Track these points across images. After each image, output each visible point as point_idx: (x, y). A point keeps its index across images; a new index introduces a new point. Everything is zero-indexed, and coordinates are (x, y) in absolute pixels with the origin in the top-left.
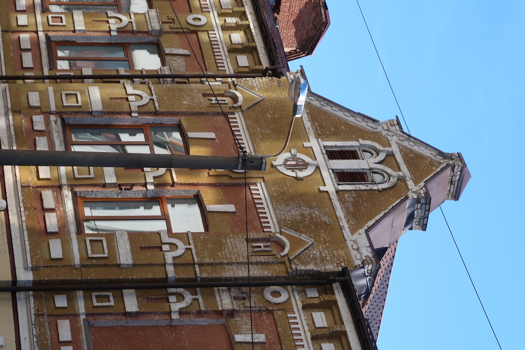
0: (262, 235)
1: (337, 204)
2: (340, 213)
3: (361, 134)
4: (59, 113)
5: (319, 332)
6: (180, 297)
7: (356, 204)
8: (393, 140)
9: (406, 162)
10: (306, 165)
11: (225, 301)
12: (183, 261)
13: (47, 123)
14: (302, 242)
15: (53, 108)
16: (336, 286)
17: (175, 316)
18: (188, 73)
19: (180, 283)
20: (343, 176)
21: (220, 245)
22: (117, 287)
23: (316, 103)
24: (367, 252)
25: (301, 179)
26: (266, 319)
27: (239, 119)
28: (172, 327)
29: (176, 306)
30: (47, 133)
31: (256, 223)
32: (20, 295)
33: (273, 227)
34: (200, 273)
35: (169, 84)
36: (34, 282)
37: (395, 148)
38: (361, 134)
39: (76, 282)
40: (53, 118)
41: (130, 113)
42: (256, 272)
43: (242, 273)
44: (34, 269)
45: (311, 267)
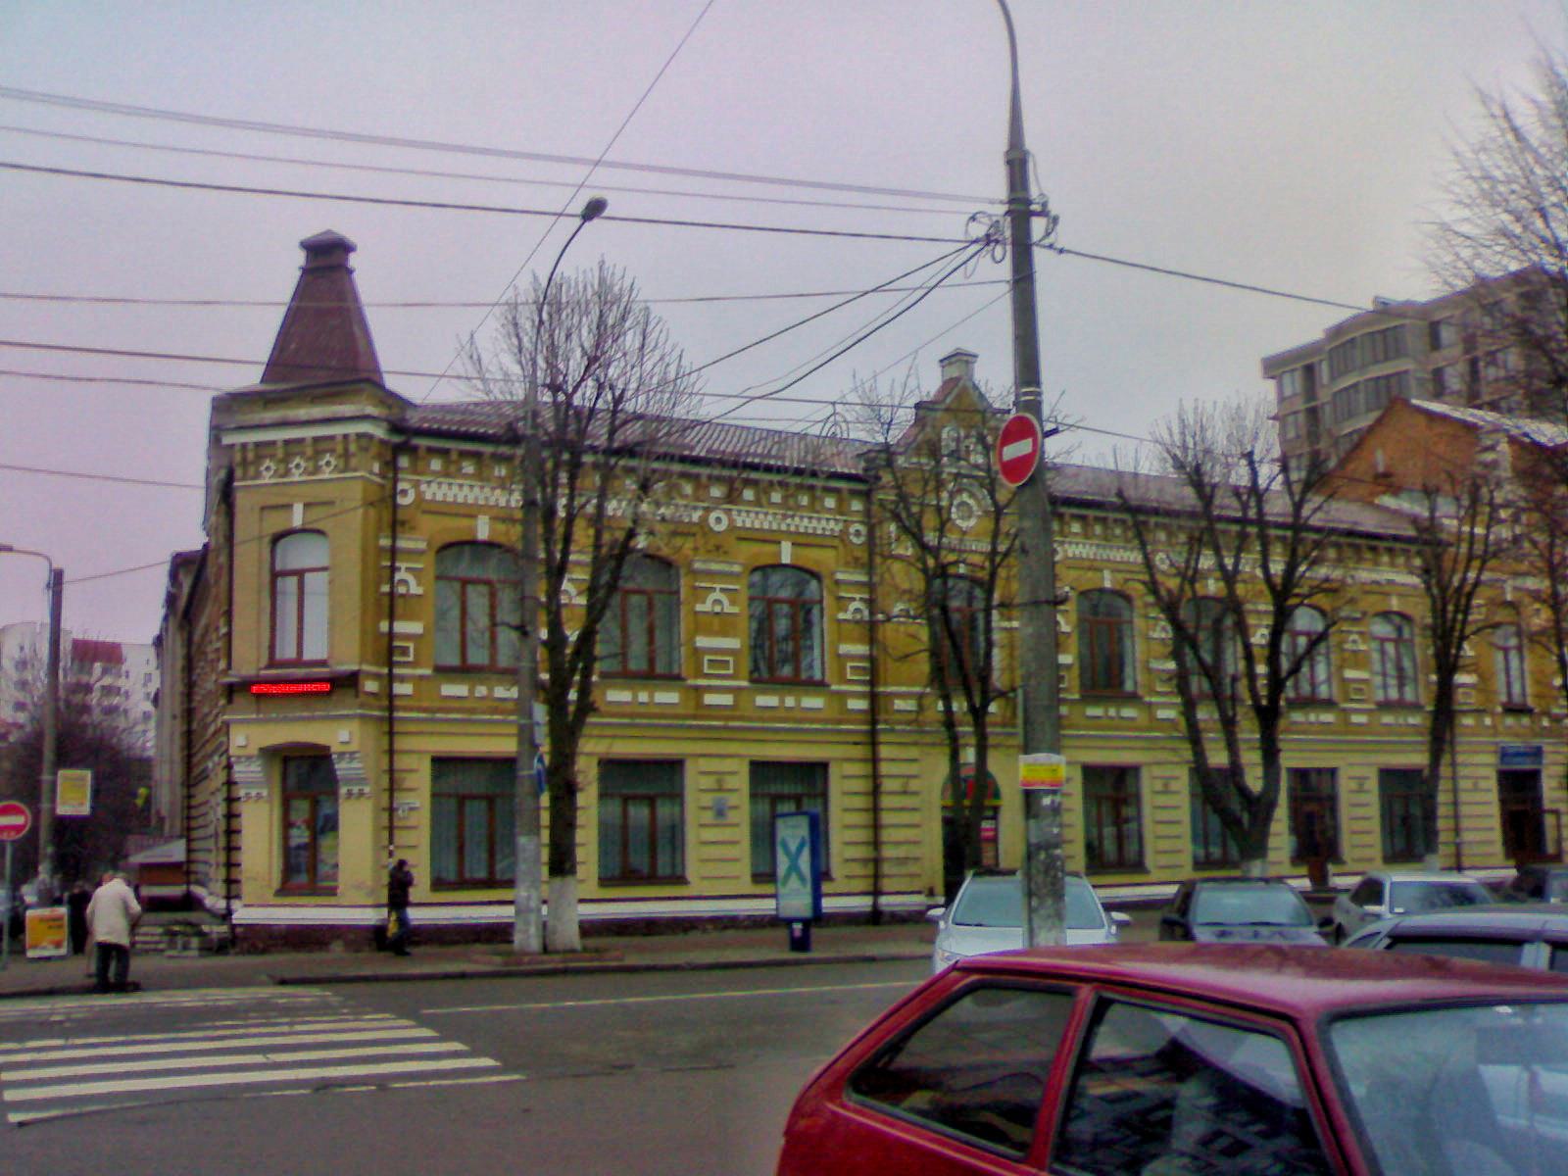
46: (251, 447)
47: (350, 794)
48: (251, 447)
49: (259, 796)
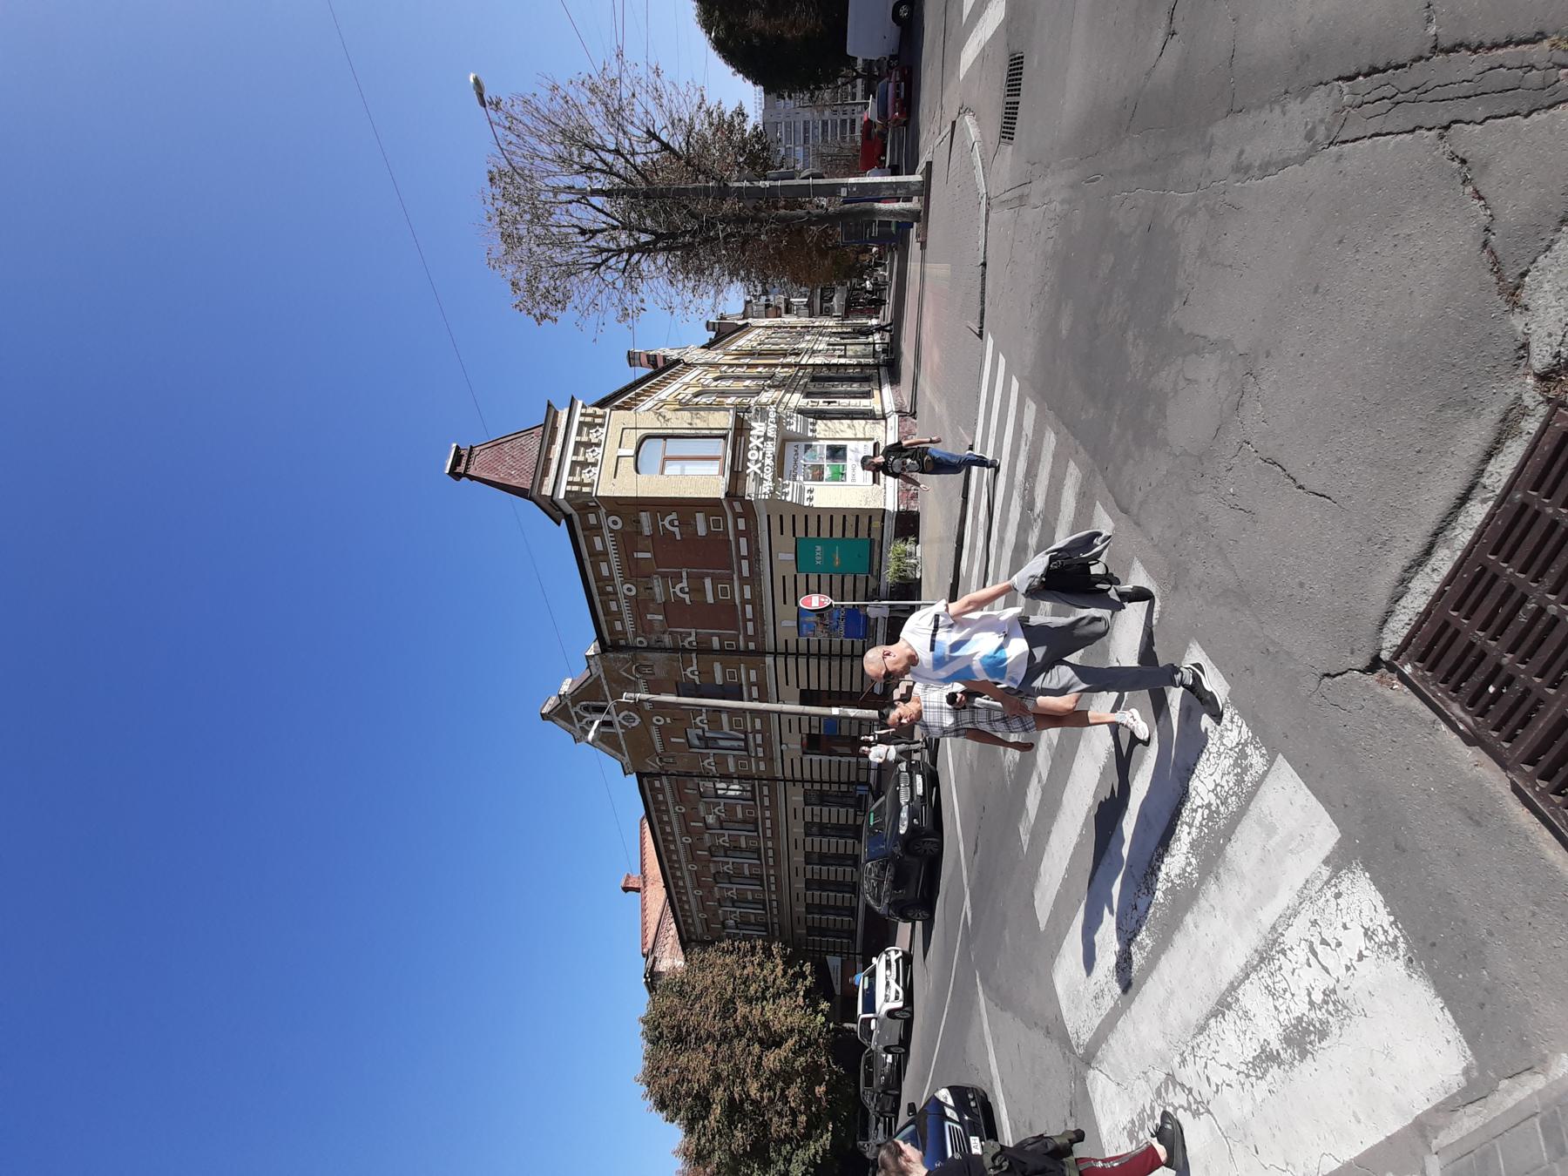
11: (667, 640)
22: (722, 651)
27: (659, 749)
30: (757, 746)
35: (695, 772)
42: (650, 655)
43: (657, 655)
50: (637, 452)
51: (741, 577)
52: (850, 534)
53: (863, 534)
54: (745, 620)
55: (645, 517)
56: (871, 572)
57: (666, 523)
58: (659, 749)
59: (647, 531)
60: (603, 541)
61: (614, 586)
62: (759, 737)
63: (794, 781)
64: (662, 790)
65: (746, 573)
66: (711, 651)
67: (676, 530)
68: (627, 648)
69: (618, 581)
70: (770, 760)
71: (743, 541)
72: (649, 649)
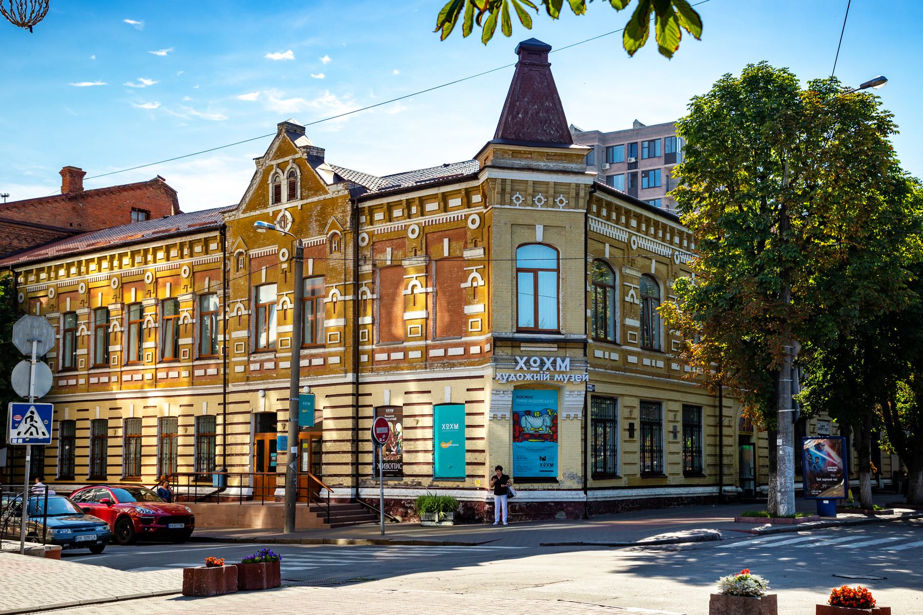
0: (328, 245)
1: (310, 200)
2: (315, 199)
3: (264, 182)
4: (249, 355)
5: (387, 217)
6: (364, 293)
7: (309, 189)
8: (268, 163)
9: (283, 157)
10: (284, 216)
11: (367, 268)
12: (343, 290)
13: (255, 362)
14: (333, 222)
15: (246, 358)
16: (361, 205)
17: (375, 296)
18: (222, 279)
19: (356, 293)
20: (292, 196)
21: (334, 269)
22: (357, 327)
23: (244, 206)
24: (340, 186)
25: (293, 221)
26: (378, 246)
27: (253, 252)
28: (381, 299)
29: (369, 296)
30: (262, 363)
31: (320, 247)
32: (361, 380)
33: (323, 238)
34: (351, 281)
35: (230, 291)
36: (354, 372)
37: (274, 163)
38: (264, 182)
39: (354, 350)
40: (252, 359)
41: (249, 315)
44: (346, 372)
45: (348, 219)
46: (508, 183)
47: (568, 417)
48: (508, 183)
49: (503, 417)
50: (540, 243)
51: (427, 348)
52: (469, 457)
53: (469, 470)
54: (389, 352)
55: (478, 253)
56: (437, 479)
57: (475, 274)
58: (253, 252)
59: (467, 254)
60: (457, 208)
61: (416, 215)
62: (270, 365)
63: (225, 404)
64: (206, 251)
65: (433, 353)
66: (357, 314)
67: (468, 284)
68: (356, 226)
69: (422, 220)
70: (247, 377)
71: (460, 351)
72: (357, 248)
